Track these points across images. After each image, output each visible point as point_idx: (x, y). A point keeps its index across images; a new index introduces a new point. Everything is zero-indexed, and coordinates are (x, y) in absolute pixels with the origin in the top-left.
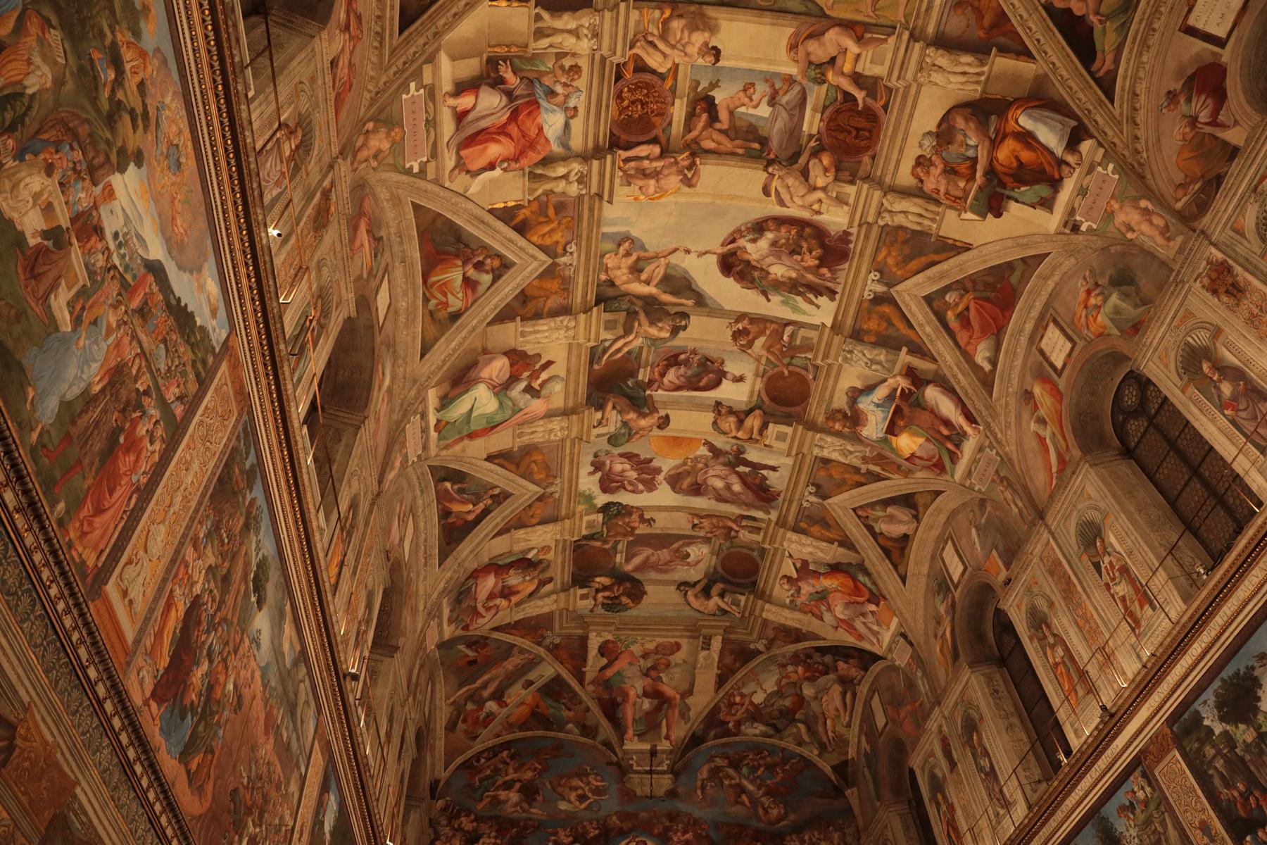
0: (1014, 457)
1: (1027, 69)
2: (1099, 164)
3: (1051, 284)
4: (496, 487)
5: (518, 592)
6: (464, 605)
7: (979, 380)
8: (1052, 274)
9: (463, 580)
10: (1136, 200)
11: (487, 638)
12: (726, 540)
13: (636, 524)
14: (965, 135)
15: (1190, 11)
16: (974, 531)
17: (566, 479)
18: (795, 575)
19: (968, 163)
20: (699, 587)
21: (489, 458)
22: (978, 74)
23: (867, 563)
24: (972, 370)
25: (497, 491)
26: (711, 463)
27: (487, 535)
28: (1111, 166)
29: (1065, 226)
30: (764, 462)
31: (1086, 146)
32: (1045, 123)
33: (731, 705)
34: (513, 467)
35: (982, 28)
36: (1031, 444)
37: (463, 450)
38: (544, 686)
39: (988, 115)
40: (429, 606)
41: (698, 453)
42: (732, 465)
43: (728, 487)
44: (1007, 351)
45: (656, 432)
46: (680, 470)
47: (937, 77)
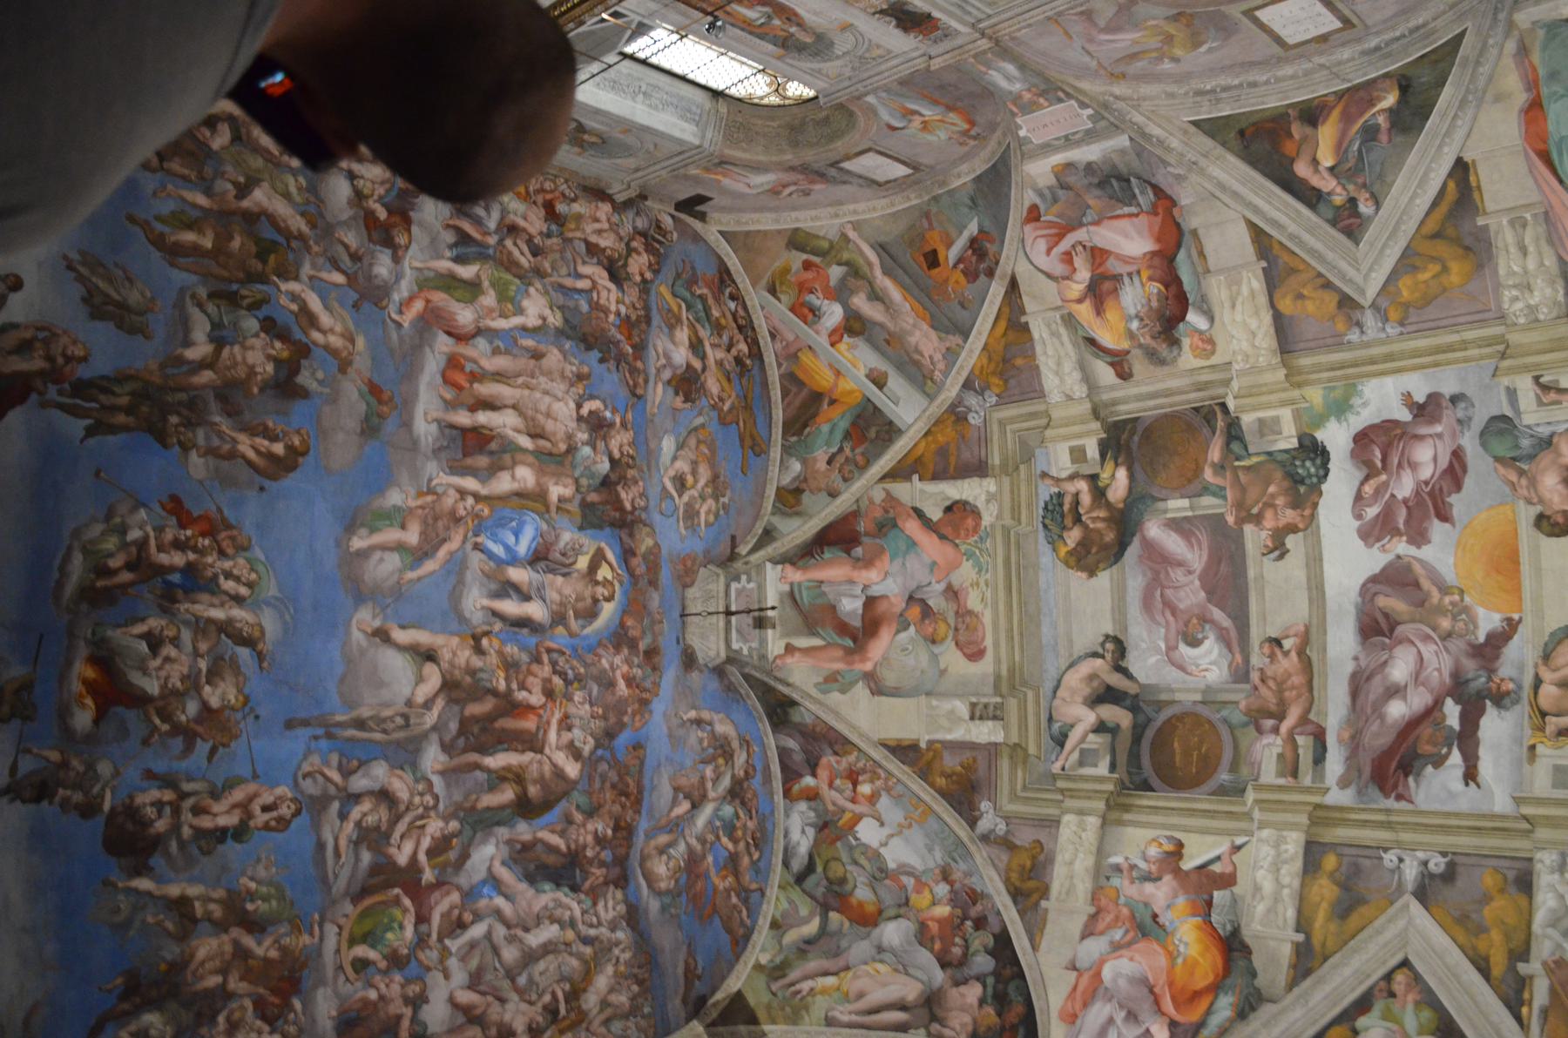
4: (1378, 205)
5: (1099, 311)
6: (1093, 200)
9: (1161, 179)
11: (990, 273)
12: (1248, 712)
13: (1269, 522)
17: (1396, 347)
18: (1188, 864)
20: (1116, 680)
21: (1461, 168)
23: (1266, 1010)
25: (1365, 208)
26: (1457, 645)
27: (1256, 210)
30: (1482, 752)
33: (853, 777)
34: (1432, 226)
37: (1498, 98)
38: (876, 408)
40: (1120, 105)
41: (1481, 612)
42: (1458, 687)
43: (1395, 691)
45: (1527, 514)
46: (1426, 584)
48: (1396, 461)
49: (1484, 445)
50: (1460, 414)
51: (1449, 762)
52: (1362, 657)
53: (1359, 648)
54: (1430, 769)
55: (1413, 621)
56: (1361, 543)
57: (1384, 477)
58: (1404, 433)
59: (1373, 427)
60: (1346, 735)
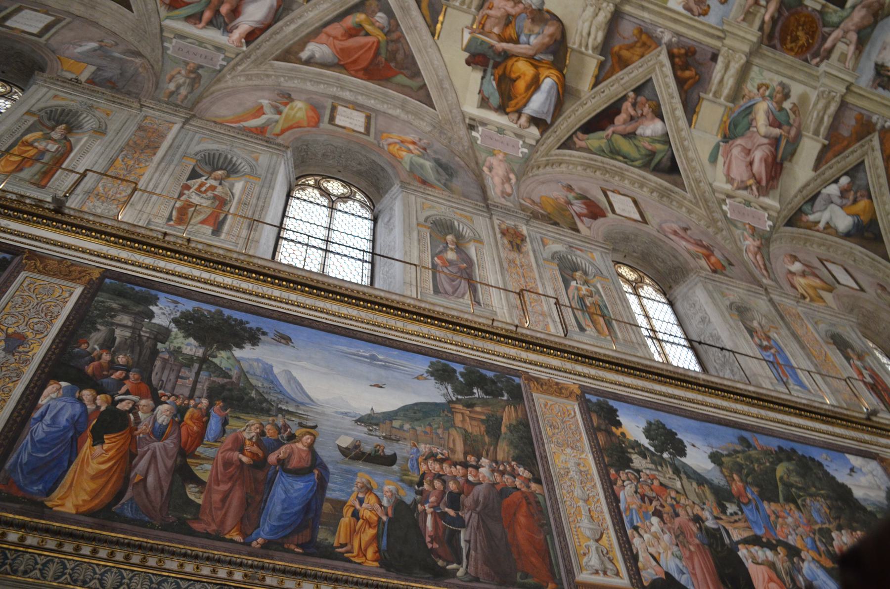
0: (222, 85)
1: (585, 85)
2: (524, 142)
3: (397, 112)
7: (290, 48)
8: (408, 112)
10: (512, 171)
14: (538, 34)
15: (613, 192)
16: (93, 45)
19: (514, 36)
22: (587, 46)
24: (301, 39)
28: (526, 150)
29: (471, 119)
31: (534, 131)
32: (547, 99)
35: (620, 49)
36: (250, 100)
39: (554, 53)
44: (321, 74)
47: (590, 11)
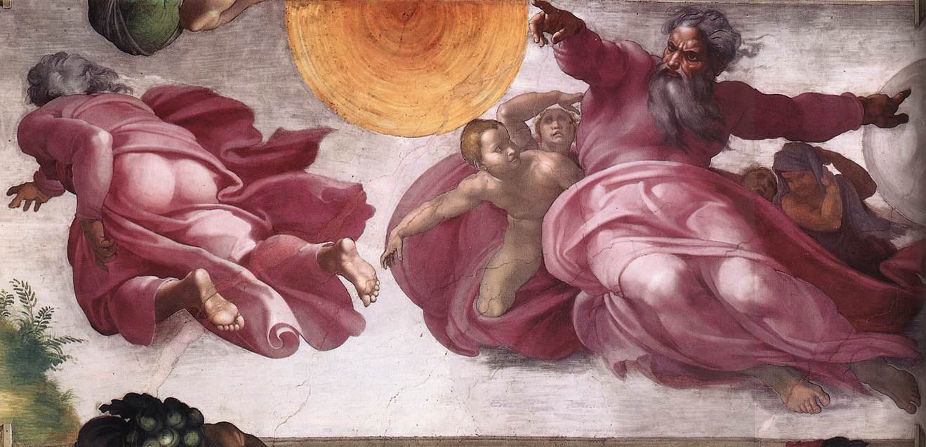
26: (595, 142)
30: (834, 87)
46: (454, 203)
48: (166, 242)
49: (149, 47)
50: (75, 86)
51: (860, 161)
52: (619, 356)
53: (600, 361)
54: (875, 201)
55: (537, 237)
56: (351, 340)
57: (201, 275)
58: (105, 218)
59: (82, 287)
60: (801, 393)
